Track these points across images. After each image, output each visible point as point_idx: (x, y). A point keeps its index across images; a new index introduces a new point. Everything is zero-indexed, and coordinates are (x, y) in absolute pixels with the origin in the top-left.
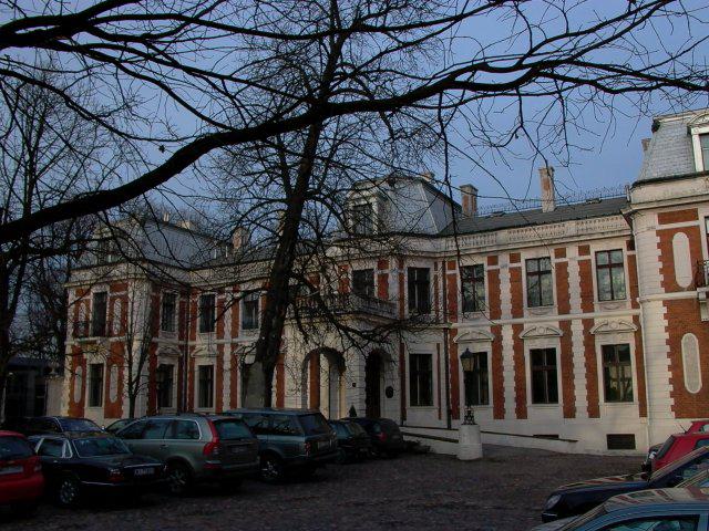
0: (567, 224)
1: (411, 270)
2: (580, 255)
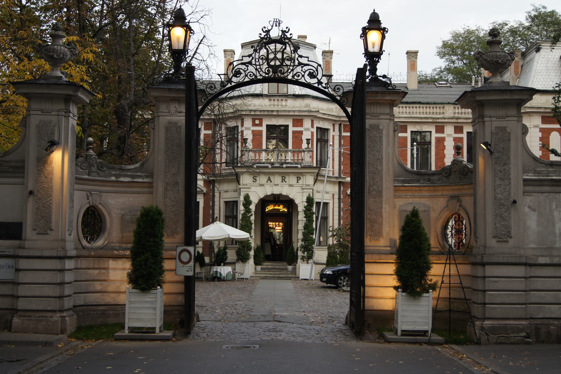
0: (447, 107)
1: (317, 128)
2: (455, 133)
